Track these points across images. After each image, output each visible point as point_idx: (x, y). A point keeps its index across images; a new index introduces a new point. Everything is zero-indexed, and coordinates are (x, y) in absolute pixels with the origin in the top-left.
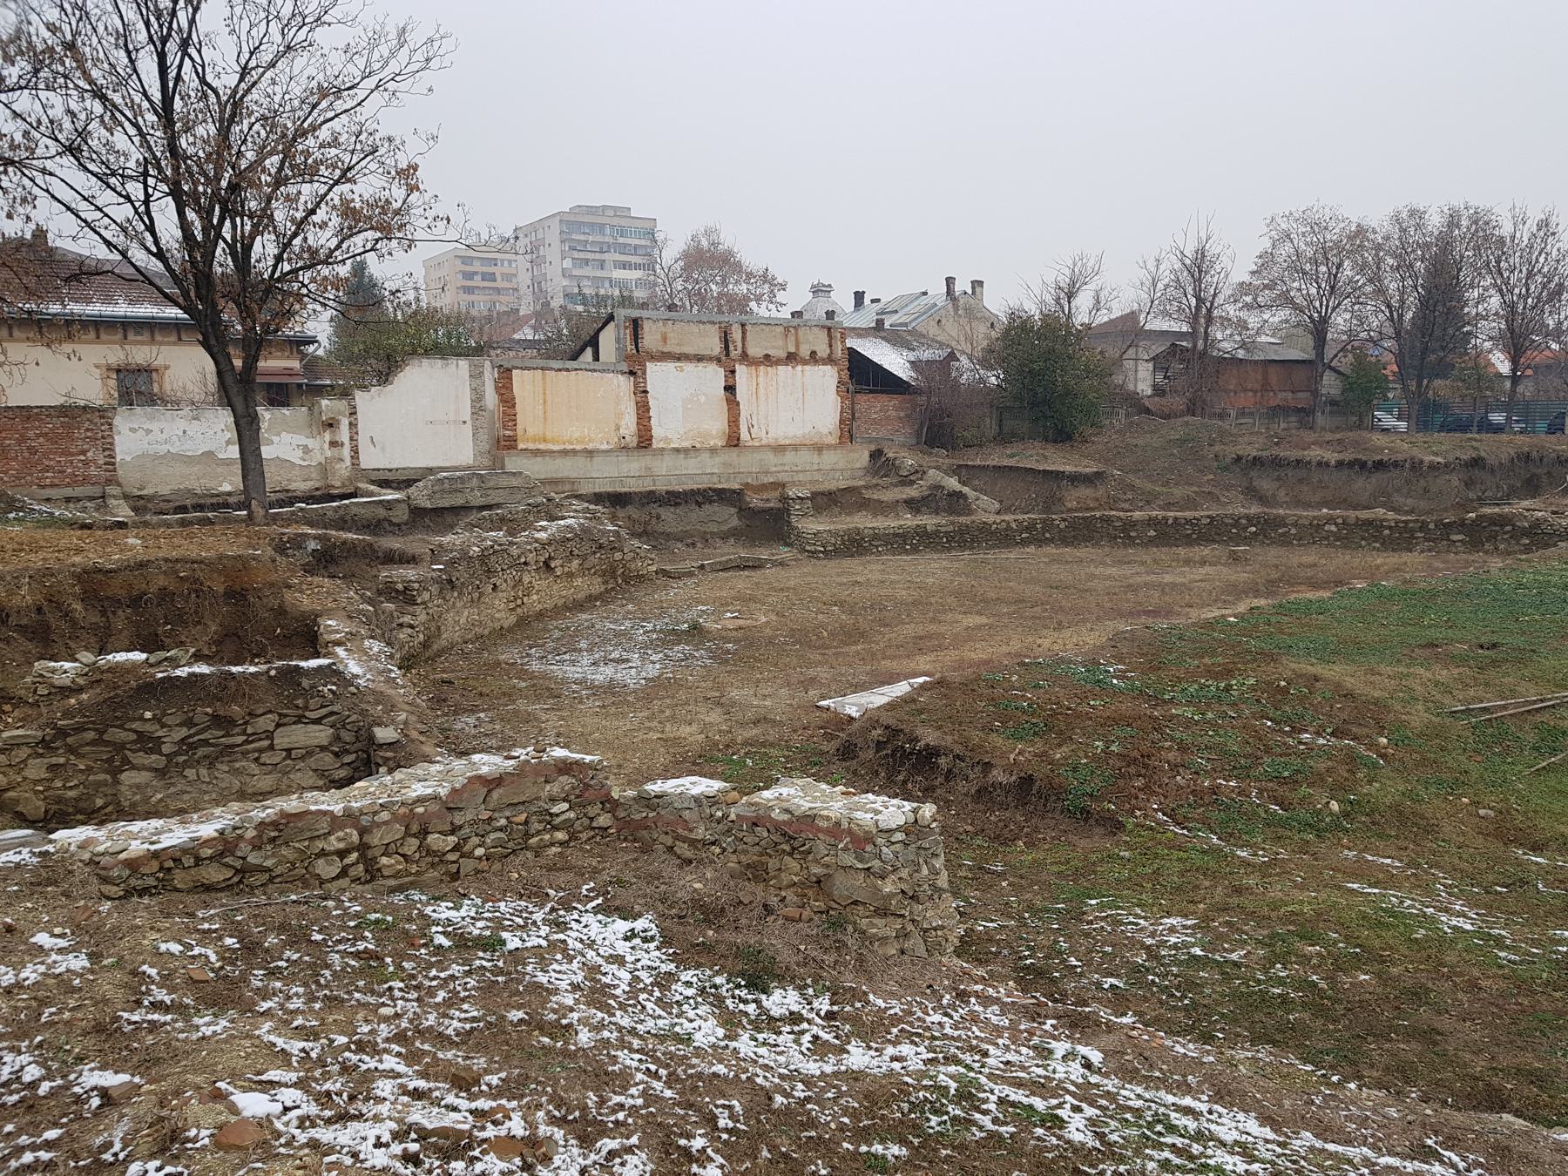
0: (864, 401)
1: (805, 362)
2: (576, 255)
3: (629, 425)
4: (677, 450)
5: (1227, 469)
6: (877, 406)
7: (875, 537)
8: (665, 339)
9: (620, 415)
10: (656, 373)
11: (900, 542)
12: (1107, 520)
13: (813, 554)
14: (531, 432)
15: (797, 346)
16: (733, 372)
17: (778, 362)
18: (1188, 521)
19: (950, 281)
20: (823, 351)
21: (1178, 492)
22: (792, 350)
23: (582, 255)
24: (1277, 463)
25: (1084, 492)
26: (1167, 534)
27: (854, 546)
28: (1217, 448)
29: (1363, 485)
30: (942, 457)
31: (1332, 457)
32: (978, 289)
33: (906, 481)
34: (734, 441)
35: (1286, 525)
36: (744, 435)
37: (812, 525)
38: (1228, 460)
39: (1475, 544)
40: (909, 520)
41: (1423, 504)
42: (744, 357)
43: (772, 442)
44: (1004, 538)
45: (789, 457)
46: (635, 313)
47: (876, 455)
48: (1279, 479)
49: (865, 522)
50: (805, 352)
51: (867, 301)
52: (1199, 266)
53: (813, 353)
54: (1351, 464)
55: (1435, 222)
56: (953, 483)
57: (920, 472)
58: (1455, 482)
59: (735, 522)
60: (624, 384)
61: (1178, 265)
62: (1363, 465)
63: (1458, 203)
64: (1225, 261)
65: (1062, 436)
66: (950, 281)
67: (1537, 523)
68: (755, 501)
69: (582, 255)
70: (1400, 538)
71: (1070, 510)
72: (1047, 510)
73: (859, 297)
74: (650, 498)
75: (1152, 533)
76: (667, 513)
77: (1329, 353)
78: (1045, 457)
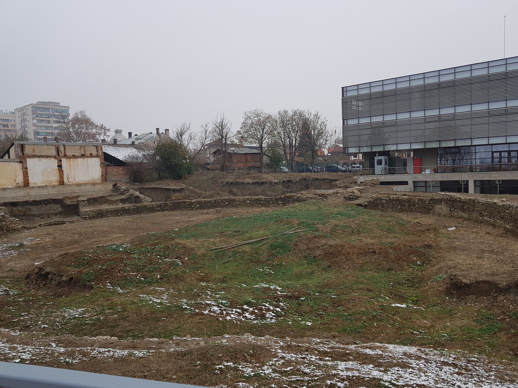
0: (110, 169)
1: (88, 157)
2: (38, 118)
3: (20, 179)
4: (39, 187)
5: (224, 186)
6: (114, 170)
7: (107, 212)
8: (34, 151)
9: (17, 176)
10: (30, 162)
11: (116, 213)
12: (185, 202)
13: (85, 218)
15: (85, 152)
16: (61, 161)
17: (78, 157)
18: (208, 202)
19: (157, 129)
20: (94, 153)
21: (208, 193)
22: (83, 153)
23: (41, 119)
24: (237, 184)
25: (178, 194)
26: (203, 206)
27: (100, 215)
28: (222, 180)
29: (259, 189)
30: (137, 185)
31: (250, 181)
32: (167, 132)
33: (122, 194)
34: (62, 183)
35: (236, 201)
36: (66, 180)
37: (83, 209)
38: (225, 183)
39: (284, 204)
40: (120, 205)
41: (274, 194)
42: (65, 156)
43: (76, 183)
44: (152, 210)
45: (83, 187)
46: (22, 143)
47: (114, 186)
48: (238, 188)
49: (105, 207)
50: (88, 153)
51: (133, 135)
52: (221, 127)
53: (91, 154)
54: (256, 183)
55: (290, 113)
56: (137, 193)
57: (127, 190)
58: (281, 187)
59: (60, 209)
61: (215, 126)
62: (258, 183)
63: (296, 109)
64: (229, 125)
65: (178, 177)
66: (157, 129)
67: (298, 198)
68: (68, 202)
69: (41, 119)
70: (266, 203)
71: (173, 200)
72: (166, 200)
73: (130, 134)
74: (27, 203)
75: (198, 206)
76: (32, 208)
77: (264, 151)
78: (168, 184)
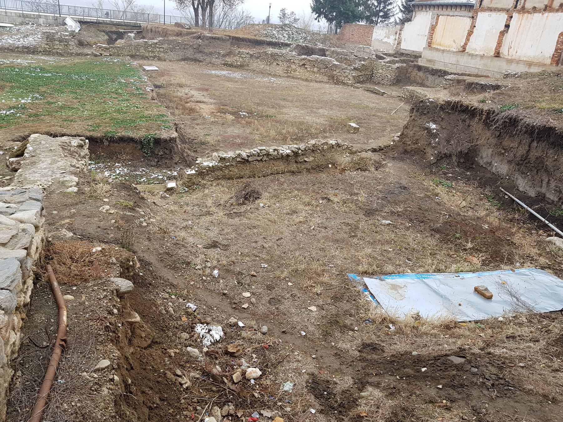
14: (438, 41)
16: (512, 17)
34: (498, 55)
36: (504, 50)
60: (468, 21)
